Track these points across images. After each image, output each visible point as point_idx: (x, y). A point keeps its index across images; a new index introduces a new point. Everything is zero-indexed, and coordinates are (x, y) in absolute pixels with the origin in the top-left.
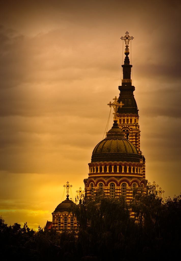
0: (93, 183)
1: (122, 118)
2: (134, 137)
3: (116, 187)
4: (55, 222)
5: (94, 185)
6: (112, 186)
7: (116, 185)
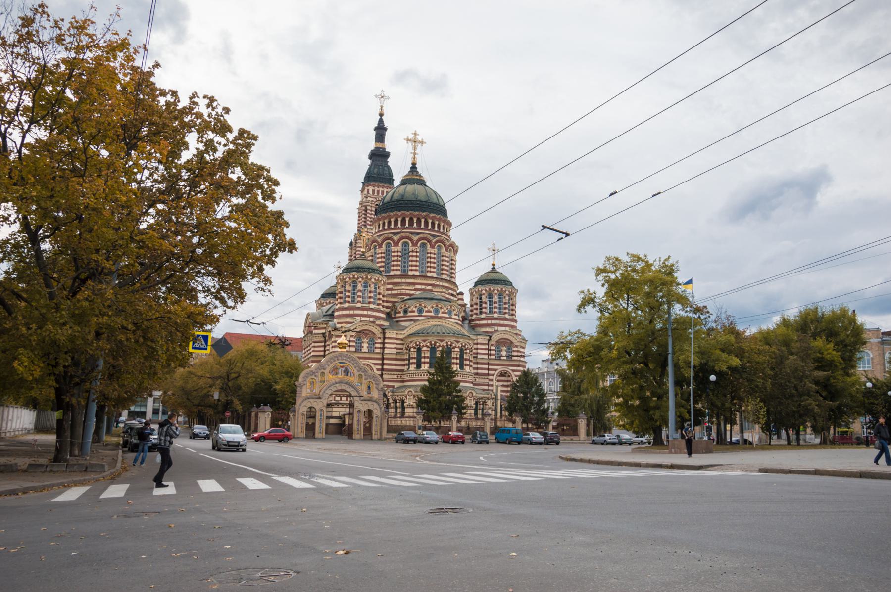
0: (391, 242)
1: (376, 189)
3: (429, 249)
5: (393, 245)
6: (423, 247)
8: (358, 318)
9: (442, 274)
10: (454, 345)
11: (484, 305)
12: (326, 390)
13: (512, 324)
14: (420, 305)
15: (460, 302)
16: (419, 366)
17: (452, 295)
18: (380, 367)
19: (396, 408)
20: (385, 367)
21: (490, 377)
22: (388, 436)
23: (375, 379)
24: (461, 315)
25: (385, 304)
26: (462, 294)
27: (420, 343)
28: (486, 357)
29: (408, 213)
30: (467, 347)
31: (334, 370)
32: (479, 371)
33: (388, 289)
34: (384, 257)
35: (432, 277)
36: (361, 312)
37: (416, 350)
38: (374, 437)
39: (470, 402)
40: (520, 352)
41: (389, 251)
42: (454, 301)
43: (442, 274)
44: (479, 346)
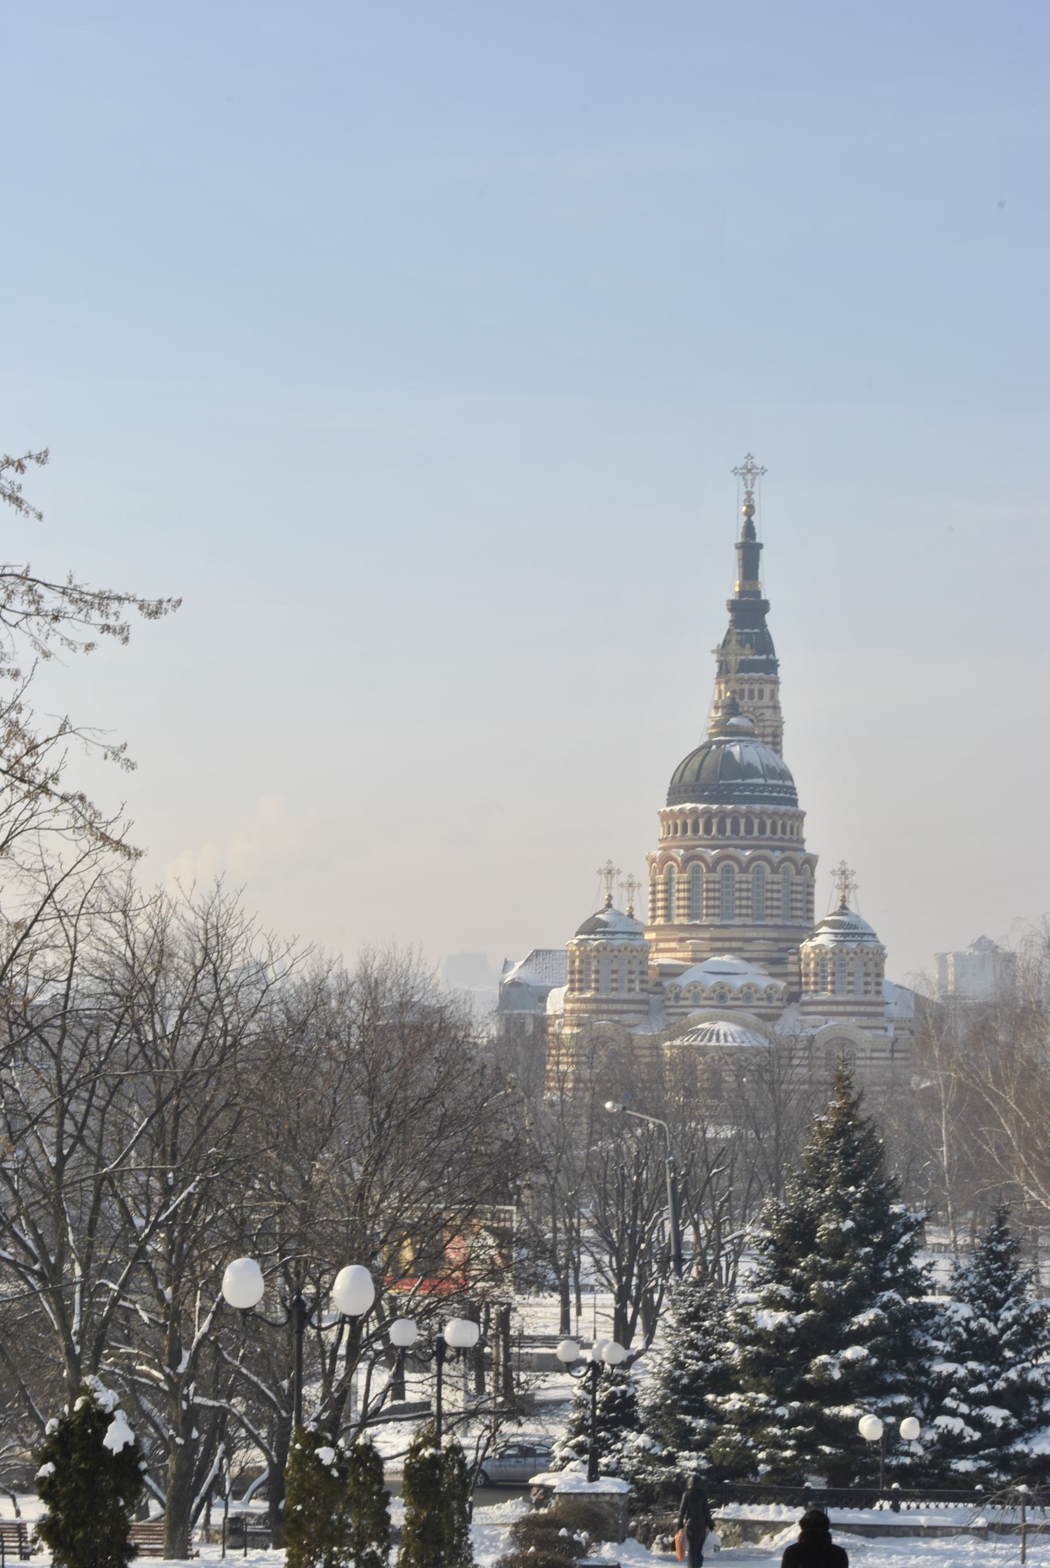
2: (770, 739)
3: (738, 877)
6: (728, 872)
7: (737, 869)
40: (871, 1058)
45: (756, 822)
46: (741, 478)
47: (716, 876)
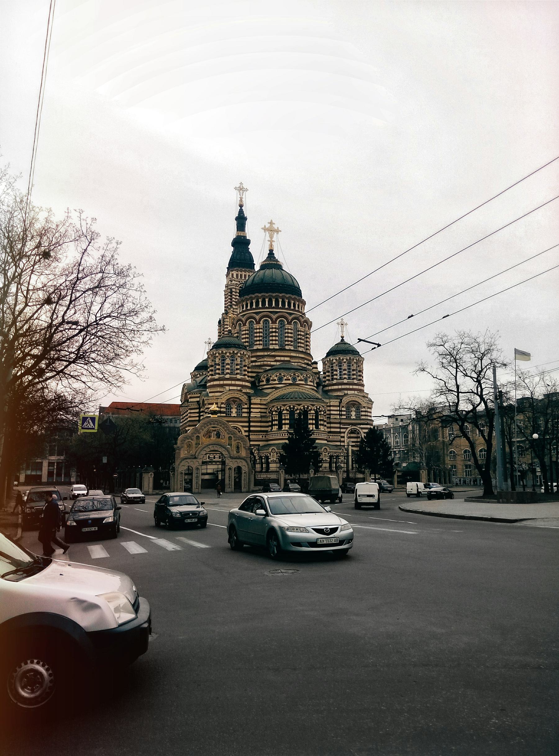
0: (254, 320)
1: (239, 273)
3: (287, 326)
4: (217, 362)
8: (227, 388)
9: (299, 346)
10: (310, 408)
11: (335, 373)
12: (201, 451)
13: (360, 387)
14: (280, 374)
15: (314, 370)
16: (280, 428)
17: (308, 364)
18: (247, 429)
19: (262, 464)
20: (252, 429)
21: (342, 435)
22: (255, 489)
23: (243, 440)
24: (315, 382)
25: (250, 374)
26: (316, 363)
27: (281, 407)
28: (338, 417)
29: (267, 295)
30: (321, 409)
31: (207, 434)
32: (332, 430)
33: (252, 362)
34: (248, 334)
35: (290, 350)
36: (229, 382)
37: (277, 413)
38: (243, 490)
39: (325, 457)
41: (252, 328)
42: (309, 370)
43: (299, 346)
44: (332, 408)
45: (293, 302)
46: (238, 191)
47: (277, 325)
